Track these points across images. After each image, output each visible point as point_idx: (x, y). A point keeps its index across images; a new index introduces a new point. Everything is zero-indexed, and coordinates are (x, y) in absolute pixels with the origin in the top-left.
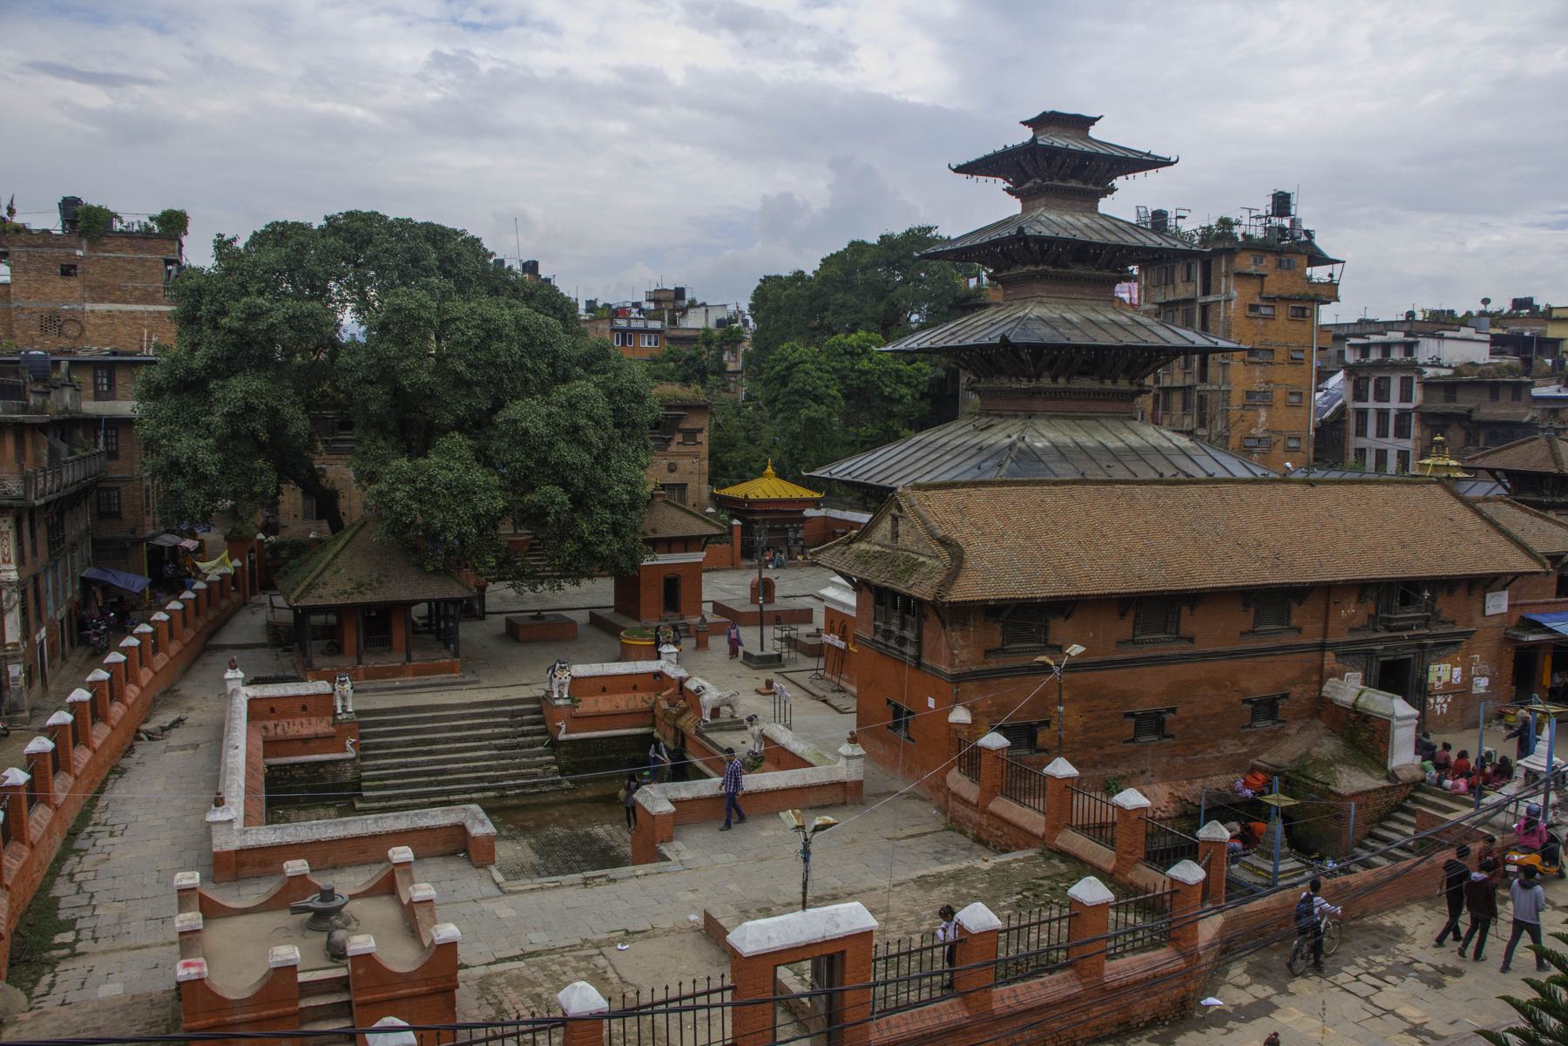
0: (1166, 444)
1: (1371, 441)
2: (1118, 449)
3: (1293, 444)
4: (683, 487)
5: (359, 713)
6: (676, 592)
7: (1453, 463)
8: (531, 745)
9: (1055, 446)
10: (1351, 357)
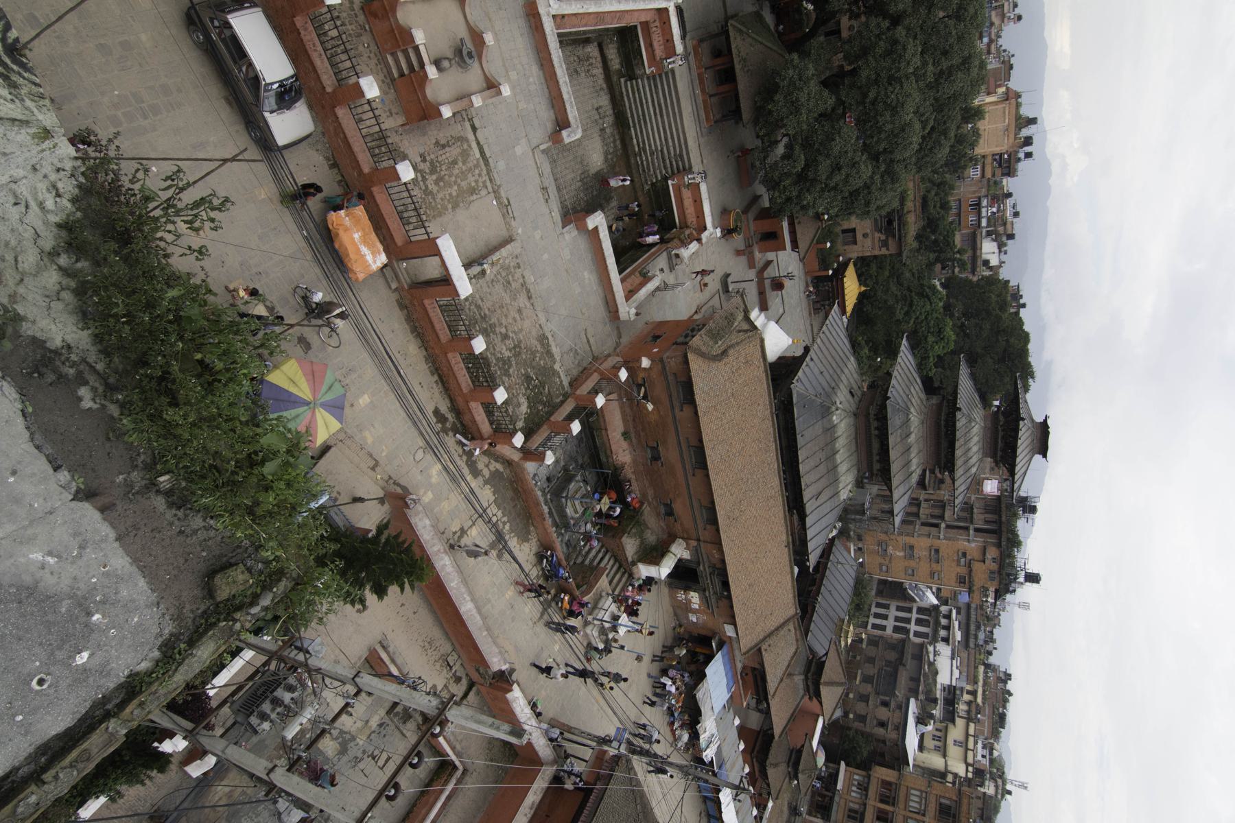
0: (841, 486)
1: (893, 613)
2: (834, 460)
3: (884, 568)
4: (855, 243)
5: (673, 71)
6: (771, 238)
8: (665, 167)
9: (834, 426)
10: (944, 609)
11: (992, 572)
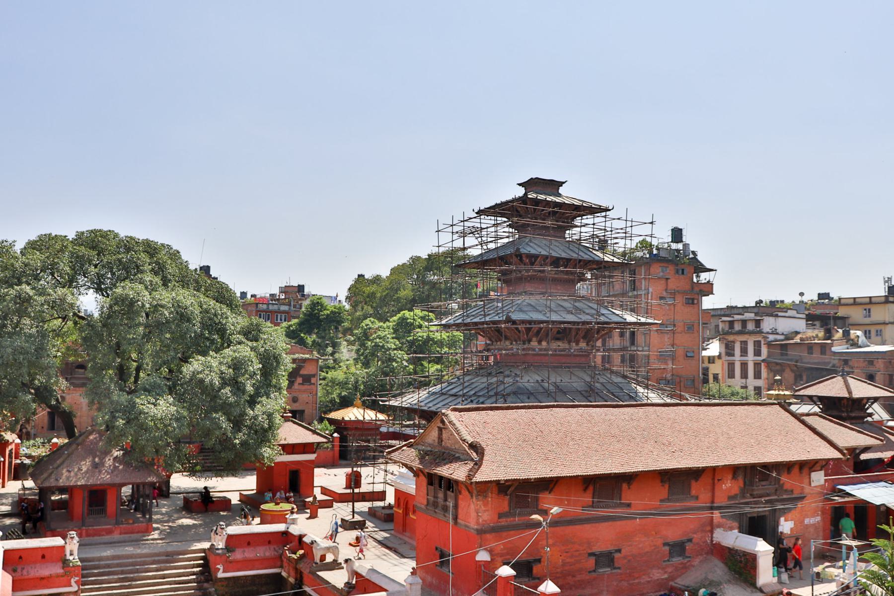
7: (787, 393)
11: (677, 272)
